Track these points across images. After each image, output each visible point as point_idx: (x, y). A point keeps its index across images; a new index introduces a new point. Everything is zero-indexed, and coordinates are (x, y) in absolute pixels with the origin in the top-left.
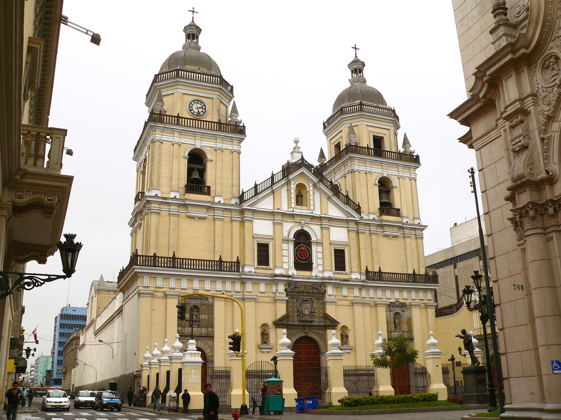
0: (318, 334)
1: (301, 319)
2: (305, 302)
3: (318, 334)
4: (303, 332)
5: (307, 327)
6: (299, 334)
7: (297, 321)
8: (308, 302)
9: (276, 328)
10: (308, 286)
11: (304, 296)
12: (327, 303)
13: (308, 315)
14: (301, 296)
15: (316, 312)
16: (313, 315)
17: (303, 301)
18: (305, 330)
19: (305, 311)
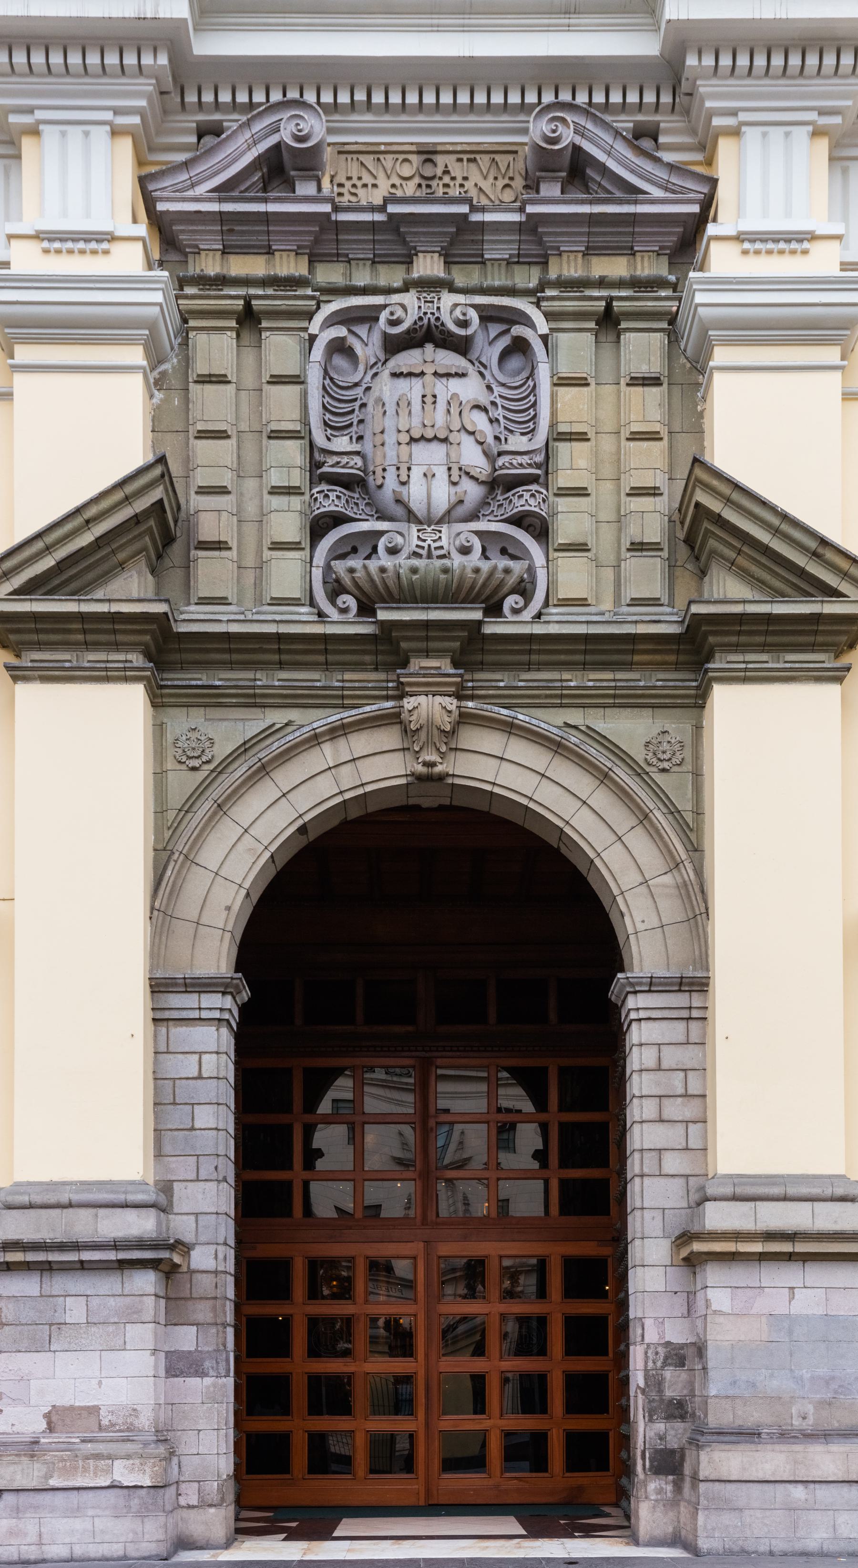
0: (593, 752)
2: (409, 359)
3: (593, 752)
4: (389, 738)
5: (445, 665)
6: (328, 753)
7: (312, 603)
8: (448, 359)
10: (471, 155)
12: (721, 356)
13: (447, 517)
15: (563, 479)
16: (519, 520)
18: (409, 703)
19: (404, 471)
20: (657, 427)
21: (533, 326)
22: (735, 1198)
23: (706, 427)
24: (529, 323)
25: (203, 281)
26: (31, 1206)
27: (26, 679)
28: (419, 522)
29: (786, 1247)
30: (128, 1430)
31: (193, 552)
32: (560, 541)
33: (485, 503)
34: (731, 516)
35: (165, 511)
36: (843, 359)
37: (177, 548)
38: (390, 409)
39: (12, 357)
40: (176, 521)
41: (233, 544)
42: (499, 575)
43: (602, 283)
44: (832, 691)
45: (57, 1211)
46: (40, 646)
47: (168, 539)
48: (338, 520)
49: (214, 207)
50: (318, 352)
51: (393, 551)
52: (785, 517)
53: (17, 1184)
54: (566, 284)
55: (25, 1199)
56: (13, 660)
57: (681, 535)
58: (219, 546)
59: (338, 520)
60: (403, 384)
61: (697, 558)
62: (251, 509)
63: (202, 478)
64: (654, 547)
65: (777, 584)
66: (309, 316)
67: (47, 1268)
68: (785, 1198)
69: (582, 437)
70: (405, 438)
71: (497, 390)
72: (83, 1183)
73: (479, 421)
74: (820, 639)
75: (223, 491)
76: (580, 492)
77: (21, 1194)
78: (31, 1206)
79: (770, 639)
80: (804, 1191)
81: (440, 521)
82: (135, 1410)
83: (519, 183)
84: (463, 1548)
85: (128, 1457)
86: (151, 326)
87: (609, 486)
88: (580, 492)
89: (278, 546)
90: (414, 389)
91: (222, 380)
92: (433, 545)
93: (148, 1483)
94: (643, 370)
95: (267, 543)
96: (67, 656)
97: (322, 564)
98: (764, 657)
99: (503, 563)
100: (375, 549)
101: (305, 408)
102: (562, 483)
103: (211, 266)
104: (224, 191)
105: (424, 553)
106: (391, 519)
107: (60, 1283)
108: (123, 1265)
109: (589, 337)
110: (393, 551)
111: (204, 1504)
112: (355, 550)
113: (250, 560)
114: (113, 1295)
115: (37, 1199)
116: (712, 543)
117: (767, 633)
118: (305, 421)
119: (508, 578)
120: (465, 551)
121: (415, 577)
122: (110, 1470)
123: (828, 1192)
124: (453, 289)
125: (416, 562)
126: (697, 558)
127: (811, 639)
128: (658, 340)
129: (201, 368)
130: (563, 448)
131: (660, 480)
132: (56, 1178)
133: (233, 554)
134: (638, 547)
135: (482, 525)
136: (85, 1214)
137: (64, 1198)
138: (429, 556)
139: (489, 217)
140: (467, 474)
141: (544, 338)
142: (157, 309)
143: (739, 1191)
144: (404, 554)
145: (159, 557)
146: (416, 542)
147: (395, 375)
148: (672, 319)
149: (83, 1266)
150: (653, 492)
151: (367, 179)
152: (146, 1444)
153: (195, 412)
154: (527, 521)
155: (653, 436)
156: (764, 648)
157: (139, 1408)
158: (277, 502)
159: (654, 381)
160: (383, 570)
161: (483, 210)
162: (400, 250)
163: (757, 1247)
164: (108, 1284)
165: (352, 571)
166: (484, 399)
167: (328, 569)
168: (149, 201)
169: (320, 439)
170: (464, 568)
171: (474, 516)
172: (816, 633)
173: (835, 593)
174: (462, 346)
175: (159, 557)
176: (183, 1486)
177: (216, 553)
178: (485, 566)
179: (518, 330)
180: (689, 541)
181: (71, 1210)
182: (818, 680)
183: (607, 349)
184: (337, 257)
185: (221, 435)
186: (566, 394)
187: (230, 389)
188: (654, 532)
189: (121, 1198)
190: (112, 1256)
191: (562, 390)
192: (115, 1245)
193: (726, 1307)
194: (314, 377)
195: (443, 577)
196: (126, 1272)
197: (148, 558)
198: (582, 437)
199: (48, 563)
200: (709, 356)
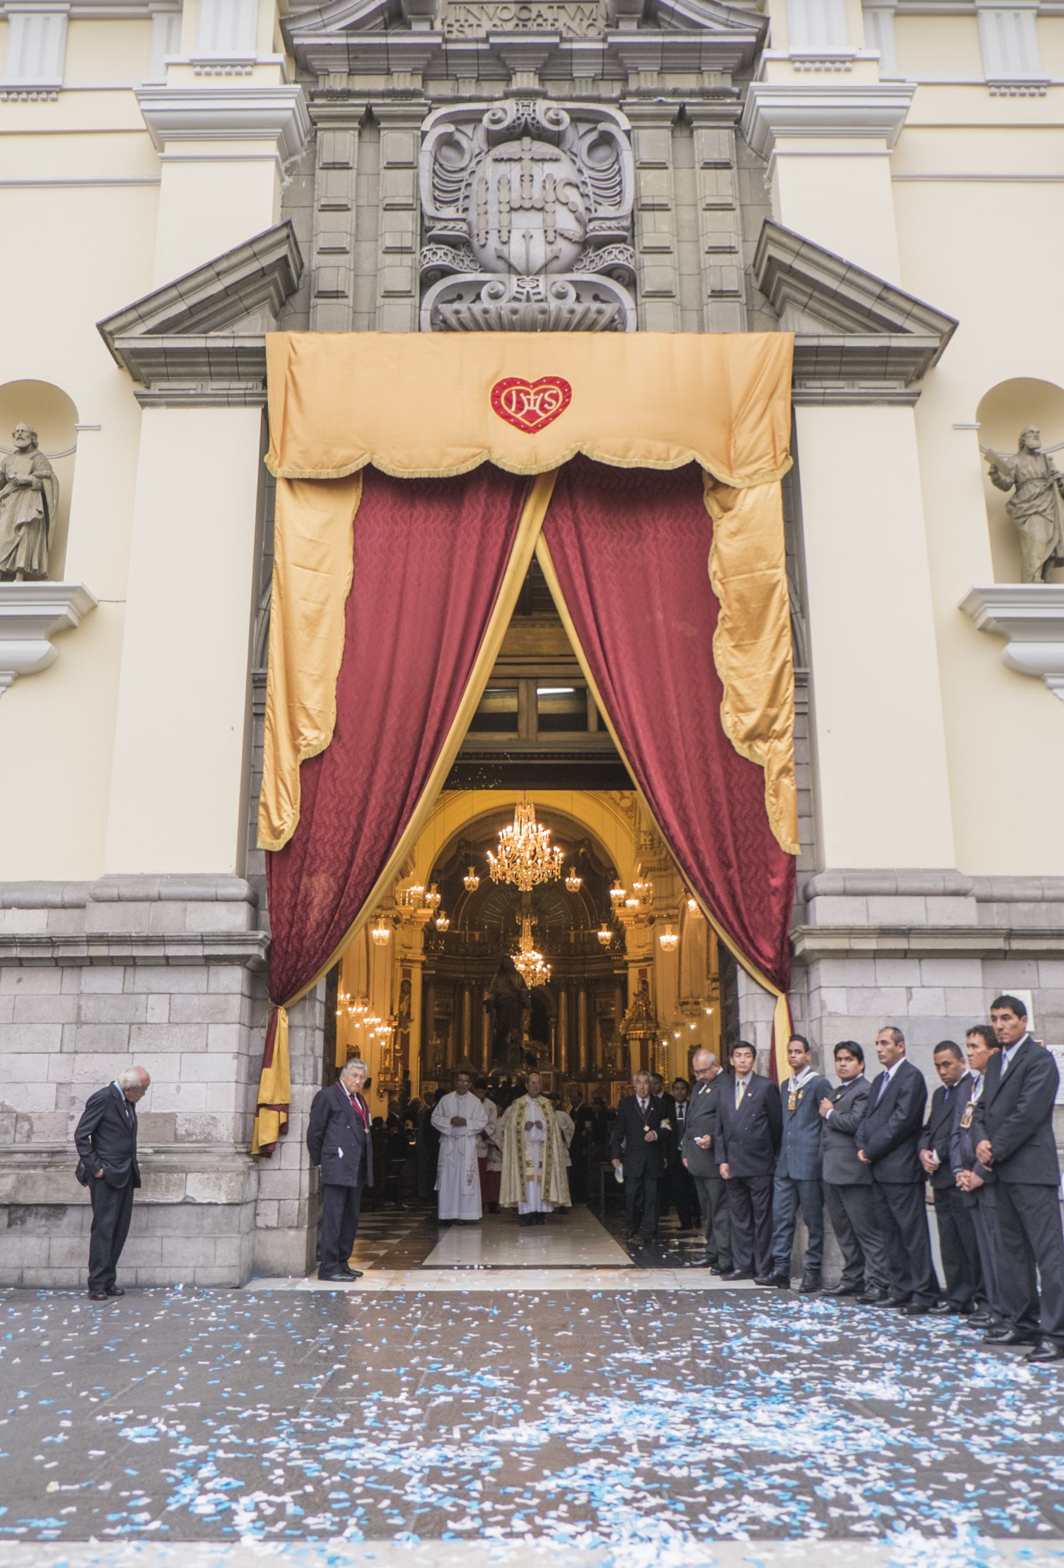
1: (447, 310)
9: (145, 401)
11: (506, 96)
12: (781, 145)
13: (544, 269)
14: (470, 100)
16: (609, 272)
17: (494, 139)
20: (730, 200)
21: (617, 124)
22: (845, 893)
23: (773, 201)
24: (612, 120)
25: (330, 94)
26: (119, 899)
27: (153, 405)
28: (518, 273)
29: (901, 944)
30: (206, 1140)
31: (313, 301)
32: (648, 289)
33: (578, 259)
34: (800, 266)
35: (288, 266)
36: (889, 148)
37: (298, 299)
38: (493, 186)
39: (162, 150)
40: (299, 276)
41: (350, 293)
42: (593, 315)
43: (675, 93)
44: (907, 412)
45: (146, 904)
46: (168, 377)
47: (291, 290)
48: (445, 272)
49: (343, 41)
50: (429, 144)
51: (495, 296)
52: (850, 267)
53: (107, 877)
54: (643, 94)
55: (114, 892)
56: (143, 390)
57: (757, 284)
58: (337, 294)
59: (445, 272)
60: (503, 167)
61: (773, 304)
62: (367, 266)
63: (322, 242)
64: (734, 294)
65: (848, 323)
66: (422, 118)
67: (131, 963)
68: (897, 893)
69: (663, 208)
70: (505, 208)
71: (587, 173)
72: (174, 876)
73: (573, 195)
74: (890, 369)
75: (342, 251)
76: (665, 251)
77: (110, 886)
78: (119, 899)
79: (844, 369)
80: (916, 885)
81: (538, 273)
82: (213, 1118)
83: (601, 23)
84: (566, 1279)
85: (203, 1171)
86: (285, 126)
87: (689, 246)
88: (665, 251)
89: (389, 294)
90: (514, 171)
91: (345, 166)
92: (532, 291)
93: (223, 1200)
94: (715, 157)
95: (381, 291)
96: (192, 385)
97: (430, 307)
98: (841, 384)
99: (595, 306)
100: (478, 297)
101: (417, 186)
102: (647, 242)
103: (338, 83)
104: (353, 28)
105: (523, 297)
106: (493, 271)
107: (144, 980)
108: (209, 961)
109: (667, 133)
110: (495, 296)
111: (283, 1226)
112: (460, 297)
113: (364, 307)
114: (198, 994)
115: (126, 892)
116: (785, 290)
117: (841, 363)
118: (417, 196)
119: (600, 317)
120: (561, 296)
121: (515, 317)
122: (183, 1185)
123: (940, 887)
124: (545, 96)
125: (515, 305)
126: (773, 304)
127: (882, 369)
128: (726, 136)
129: (326, 157)
130: (647, 217)
131: (734, 241)
132: (147, 871)
133: (350, 301)
134: (718, 294)
135: (576, 276)
136: (173, 907)
137: (153, 892)
138: (528, 300)
139: (575, 46)
140: (562, 235)
141: (628, 133)
142: (290, 113)
143: (850, 885)
144: (505, 298)
145: (282, 304)
146: (515, 288)
147: (496, 160)
148: (738, 120)
149: (168, 962)
150: (730, 250)
151: (472, 20)
152: (223, 1156)
153: (320, 190)
154: (617, 273)
155: (727, 207)
156: (839, 376)
157: (217, 1116)
158: (390, 259)
159: (726, 166)
160: (486, 311)
161: (571, 40)
162: (503, 71)
163: (871, 944)
164: (192, 981)
165: (457, 312)
166: (576, 178)
167: (436, 311)
168: (287, 38)
169: (429, 209)
170: (560, 310)
171: (569, 269)
172: (886, 363)
173: (901, 330)
174: (556, 139)
175: (282, 304)
176: (262, 1205)
177: (334, 301)
178: (580, 308)
179: (602, 126)
180: (764, 290)
181: (159, 904)
182: (892, 403)
183: (682, 141)
184: (447, 76)
185: (343, 208)
186: (648, 175)
187: (352, 173)
188: (732, 281)
189: (211, 891)
190: (198, 951)
191: (644, 172)
192: (202, 940)
193: (842, 1009)
194: (425, 163)
195: (540, 317)
196: (213, 969)
197: (272, 305)
198: (663, 208)
199: (181, 307)
200: (772, 145)
